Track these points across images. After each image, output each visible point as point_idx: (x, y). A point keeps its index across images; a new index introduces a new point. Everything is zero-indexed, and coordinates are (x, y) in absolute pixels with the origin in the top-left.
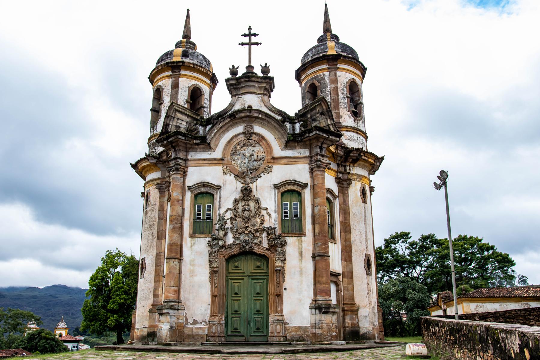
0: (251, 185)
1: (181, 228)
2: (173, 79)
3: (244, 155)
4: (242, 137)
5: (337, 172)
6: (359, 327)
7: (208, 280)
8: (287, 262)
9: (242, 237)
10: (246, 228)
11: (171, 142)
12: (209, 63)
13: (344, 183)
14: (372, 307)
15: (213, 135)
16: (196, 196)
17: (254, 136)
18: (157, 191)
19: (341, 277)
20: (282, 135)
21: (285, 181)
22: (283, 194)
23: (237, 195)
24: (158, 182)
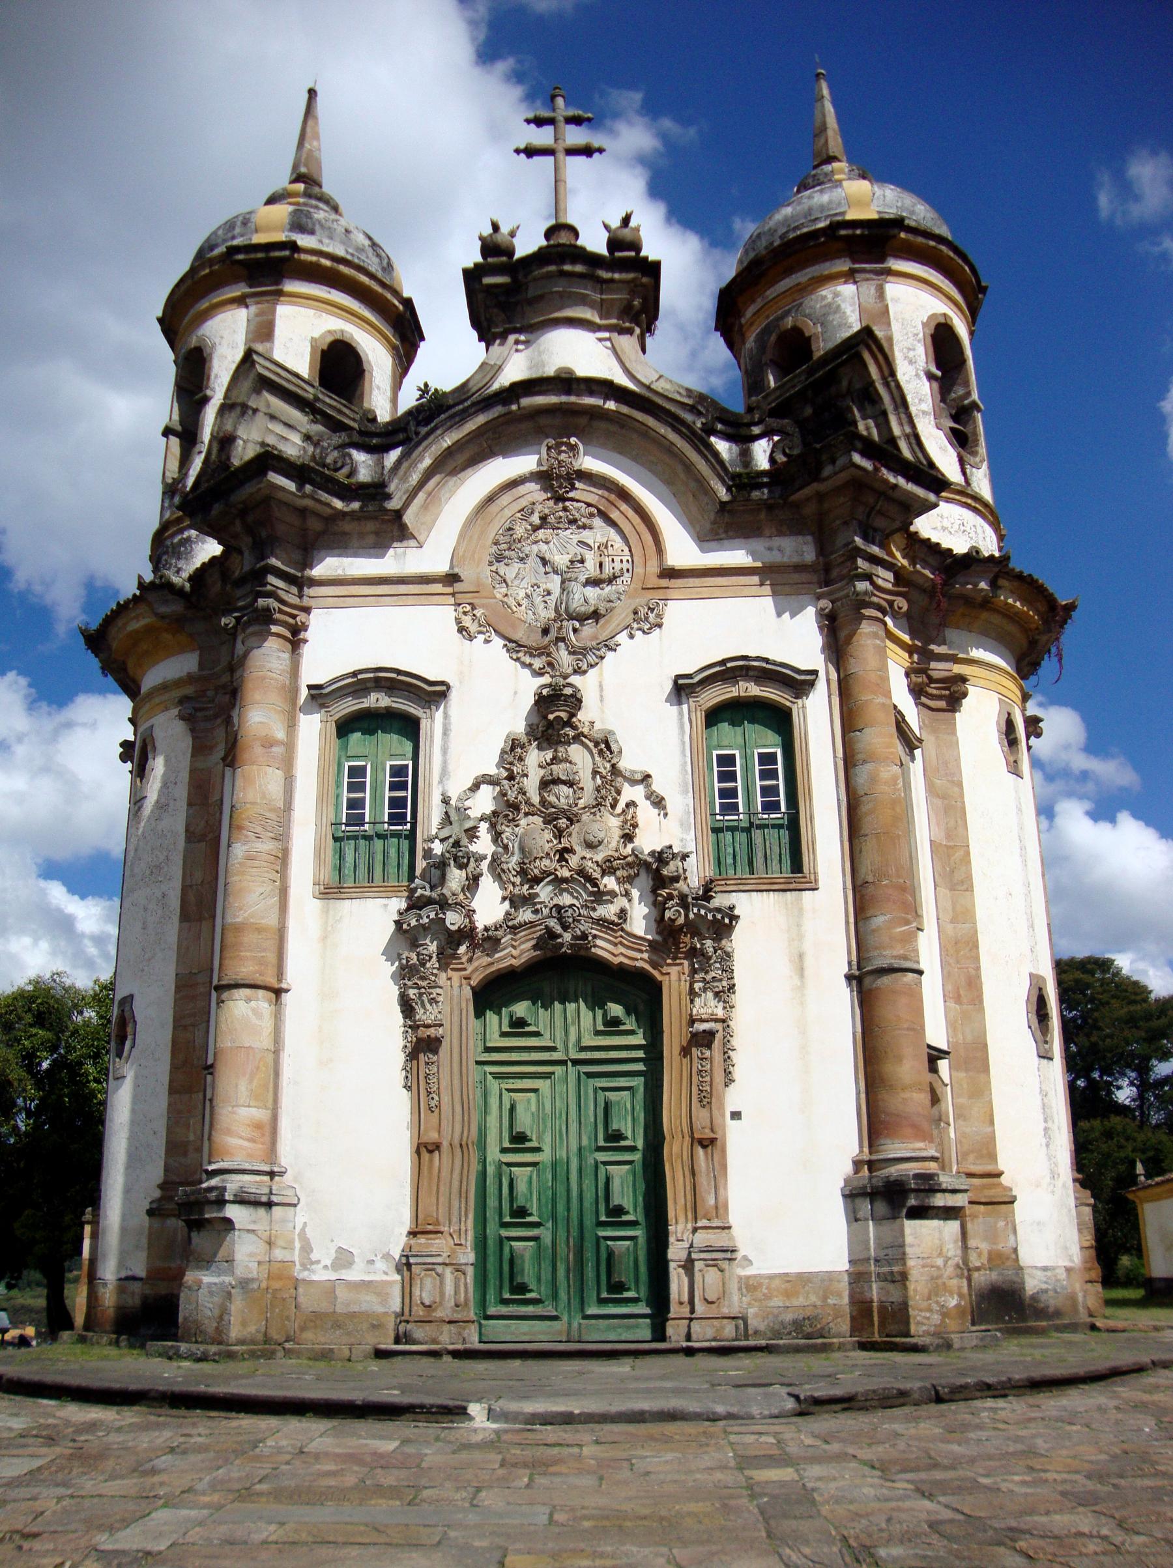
0: (575, 680)
1: (283, 859)
2: (253, 309)
4: (533, 492)
6: (1021, 1268)
7: (399, 1077)
8: (738, 998)
9: (544, 892)
10: (564, 854)
12: (389, 267)
14: (1059, 1183)
15: (415, 478)
16: (345, 728)
21: (723, 662)
22: (713, 717)
24: (189, 690)
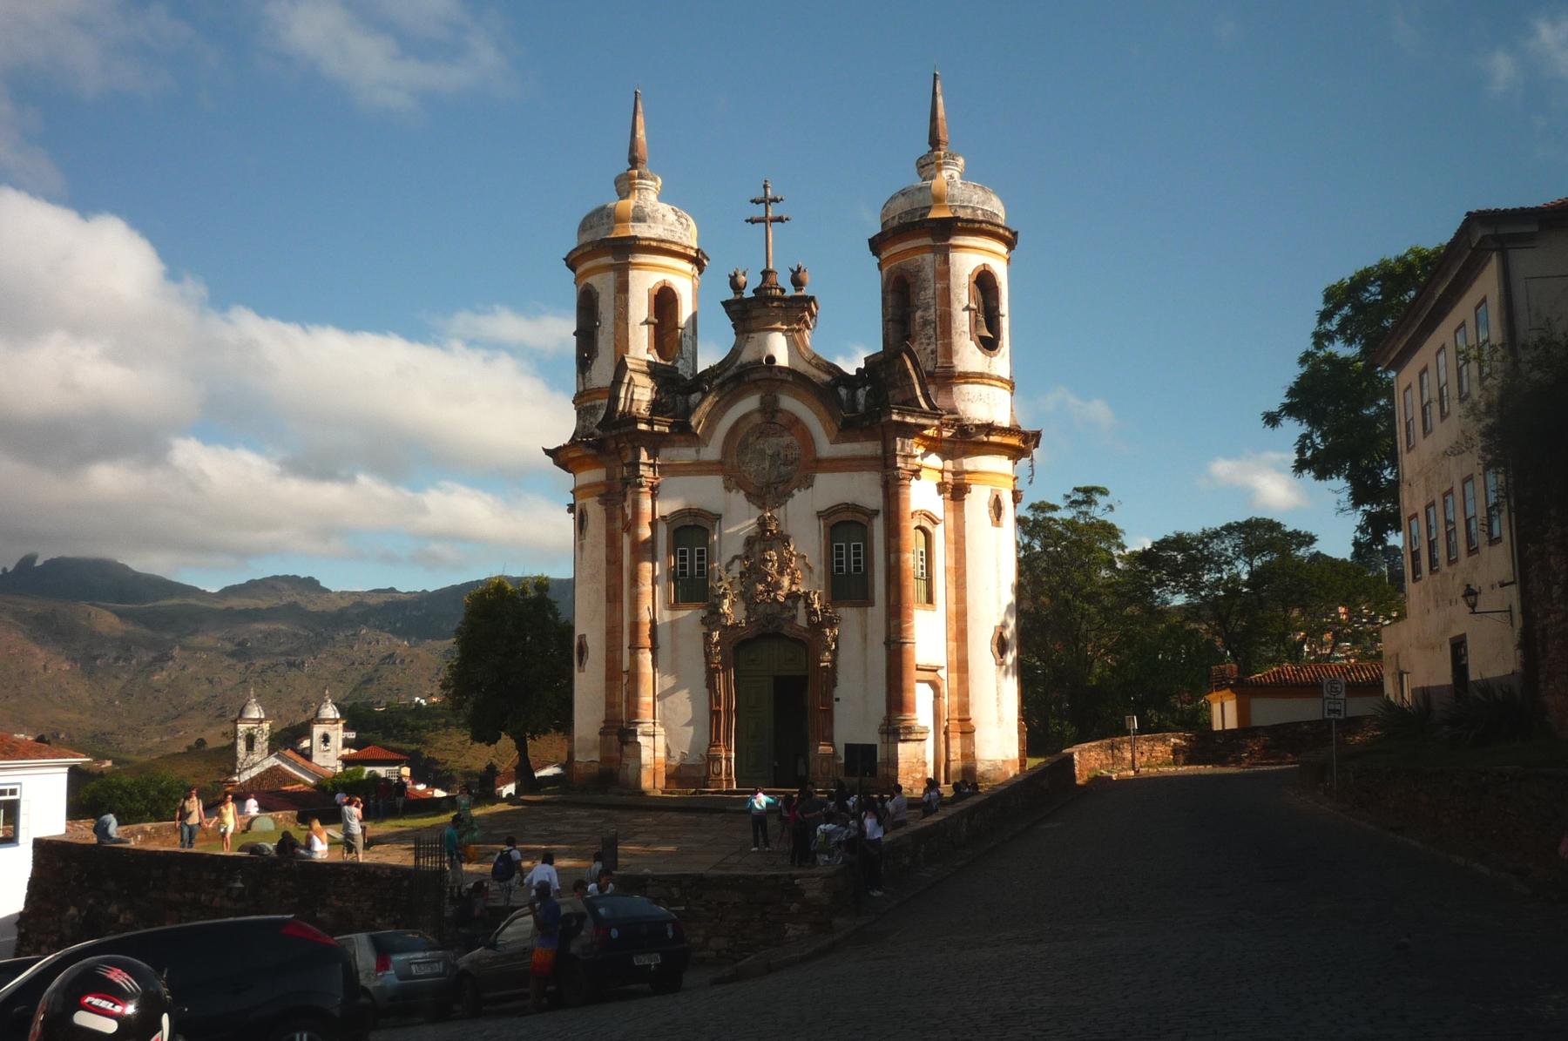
3: (762, 452)
4: (757, 419)
5: (942, 472)
7: (703, 683)
9: (760, 609)
10: (768, 592)
11: (626, 434)
13: (956, 491)
19: (943, 673)
24: (603, 490)
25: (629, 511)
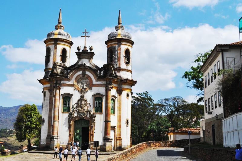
4: (81, 76)
5: (118, 88)
8: (95, 123)
9: (80, 114)
10: (82, 110)
15: (70, 75)
17: (86, 75)
18: (48, 92)
19: (116, 128)
20: (96, 76)
23: (79, 98)
24: (49, 88)
25: (54, 93)
